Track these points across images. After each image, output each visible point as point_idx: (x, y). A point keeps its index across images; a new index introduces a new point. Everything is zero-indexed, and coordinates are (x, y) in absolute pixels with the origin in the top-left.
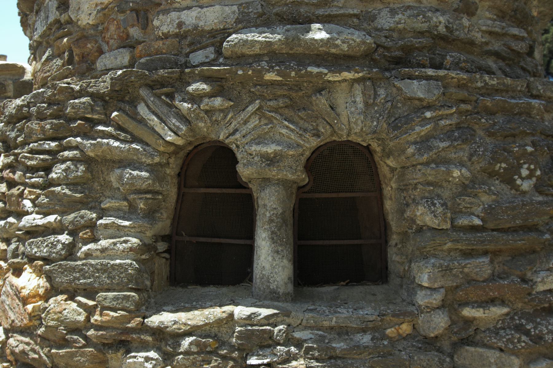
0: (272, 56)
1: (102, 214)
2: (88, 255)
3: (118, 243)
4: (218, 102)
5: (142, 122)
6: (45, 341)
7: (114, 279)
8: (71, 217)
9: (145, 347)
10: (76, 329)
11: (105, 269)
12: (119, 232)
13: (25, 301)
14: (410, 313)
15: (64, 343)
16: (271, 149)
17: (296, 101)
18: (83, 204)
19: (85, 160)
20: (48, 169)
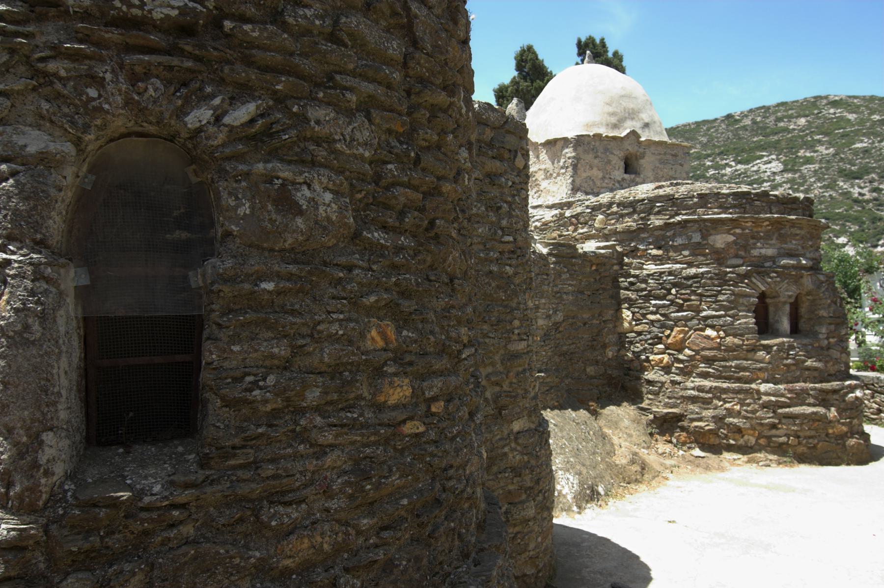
0: (794, 267)
1: (740, 311)
2: (739, 324)
3: (748, 320)
4: (778, 279)
5: (754, 283)
6: (725, 351)
7: (749, 331)
8: (732, 312)
9: (760, 350)
10: (738, 346)
11: (747, 328)
12: (746, 317)
13: (713, 339)
14: (818, 340)
15: (735, 350)
16: (790, 293)
17: (797, 280)
18: (733, 309)
19: (733, 294)
20: (716, 296)
